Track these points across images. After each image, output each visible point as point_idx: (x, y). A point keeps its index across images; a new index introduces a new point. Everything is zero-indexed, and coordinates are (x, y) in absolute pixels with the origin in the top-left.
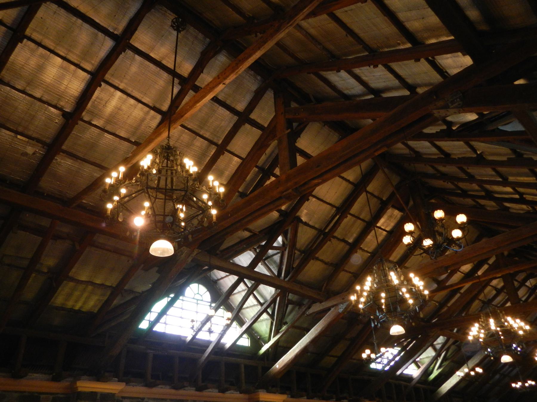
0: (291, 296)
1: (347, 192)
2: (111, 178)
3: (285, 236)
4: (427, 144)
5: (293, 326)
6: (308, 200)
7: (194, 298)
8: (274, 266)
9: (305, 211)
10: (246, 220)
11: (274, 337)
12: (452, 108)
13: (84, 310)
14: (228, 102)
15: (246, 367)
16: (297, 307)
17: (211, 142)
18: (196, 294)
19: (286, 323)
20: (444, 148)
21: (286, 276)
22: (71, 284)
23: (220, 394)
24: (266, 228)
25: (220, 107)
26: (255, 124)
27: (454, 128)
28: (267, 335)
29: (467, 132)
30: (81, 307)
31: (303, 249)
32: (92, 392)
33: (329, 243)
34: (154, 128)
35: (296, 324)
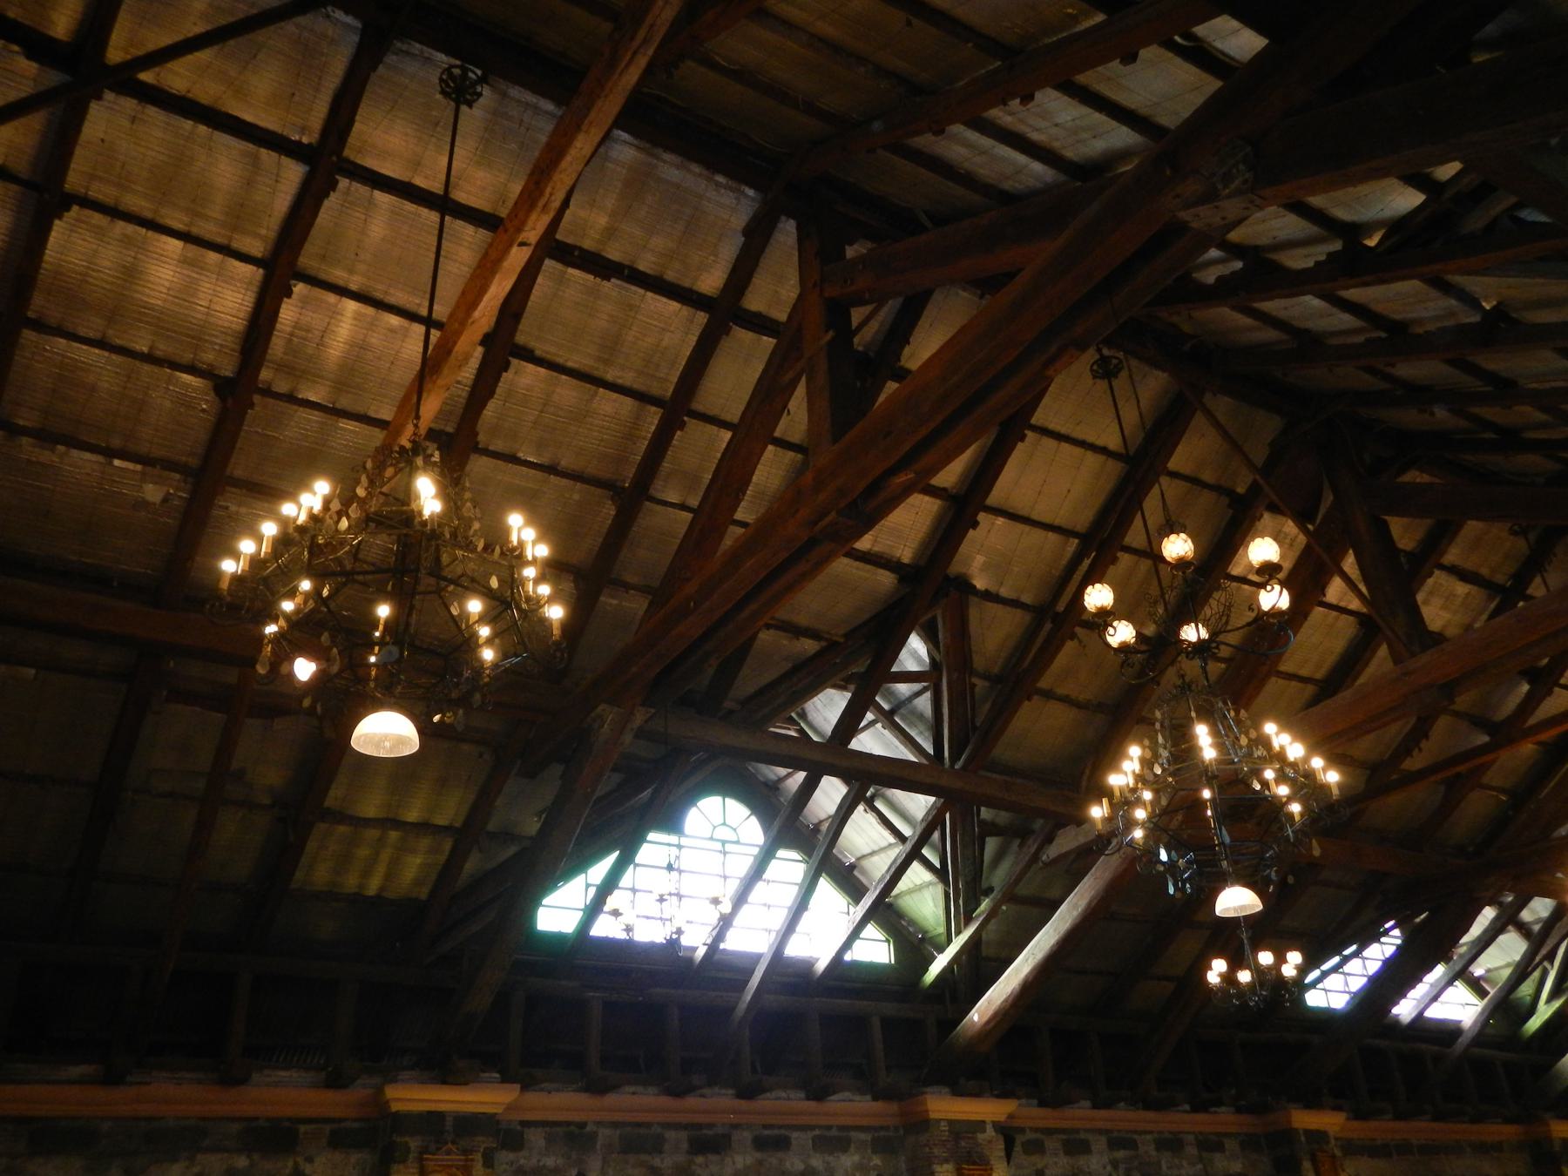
0: (986, 813)
1: (1107, 485)
2: (236, 555)
3: (930, 637)
4: (1313, 302)
5: (1010, 896)
6: (975, 525)
7: (711, 839)
8: (922, 728)
9: (979, 560)
10: (746, 613)
11: (958, 933)
12: (1229, 197)
13: (389, 895)
14: (670, 276)
15: (886, 1022)
16: (1017, 842)
17: (642, 397)
18: (719, 826)
19: (988, 891)
20: (1378, 308)
21: (954, 757)
22: (342, 829)
23: (812, 1105)
24: (865, 624)
25: (649, 294)
26: (760, 324)
27: (1372, 242)
28: (942, 929)
29: (1410, 245)
30: (382, 889)
31: (996, 670)
32: (430, 1113)
33: (1070, 646)
34: (470, 382)
35: (1022, 890)
